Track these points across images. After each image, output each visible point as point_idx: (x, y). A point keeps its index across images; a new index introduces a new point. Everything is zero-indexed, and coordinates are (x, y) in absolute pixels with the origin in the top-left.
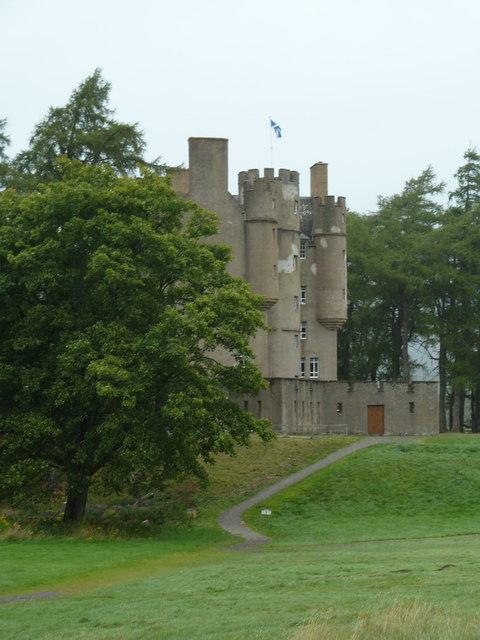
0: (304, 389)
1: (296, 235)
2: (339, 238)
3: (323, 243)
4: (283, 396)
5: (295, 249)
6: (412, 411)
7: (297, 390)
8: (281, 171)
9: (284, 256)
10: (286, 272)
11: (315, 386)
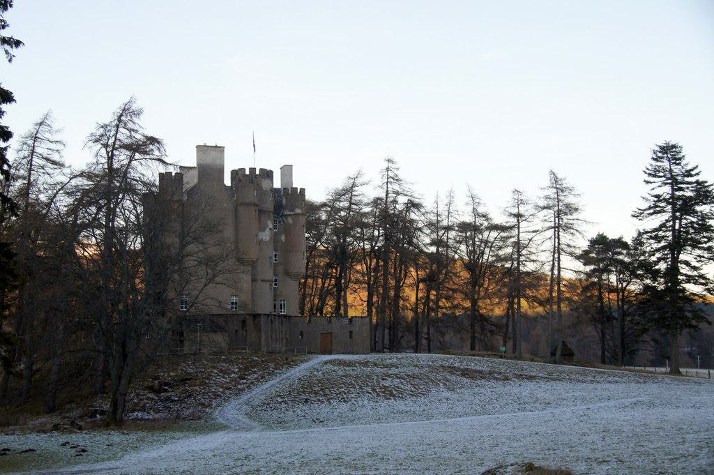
0: (277, 324)
2: (301, 217)
5: (270, 225)
6: (351, 337)
7: (272, 322)
9: (263, 230)
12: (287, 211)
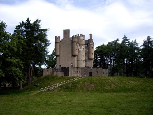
1: (83, 45)
3: (89, 46)
8: (80, 35)
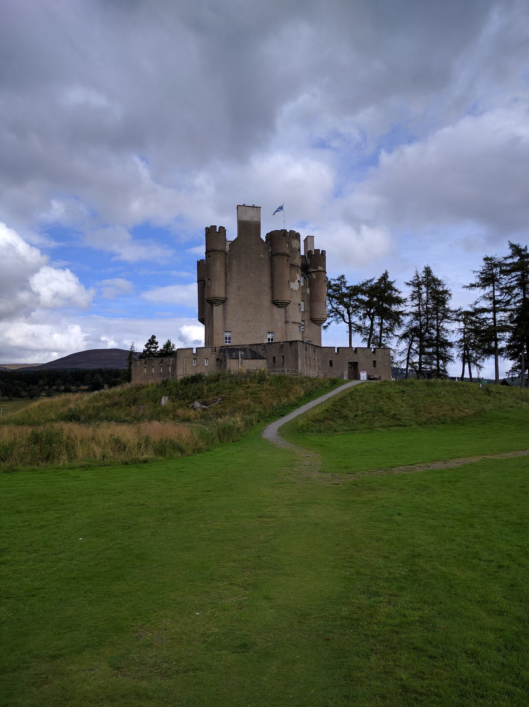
4: (299, 352)
6: (375, 366)
10: (294, 289)
11: (316, 348)
12: (311, 269)
